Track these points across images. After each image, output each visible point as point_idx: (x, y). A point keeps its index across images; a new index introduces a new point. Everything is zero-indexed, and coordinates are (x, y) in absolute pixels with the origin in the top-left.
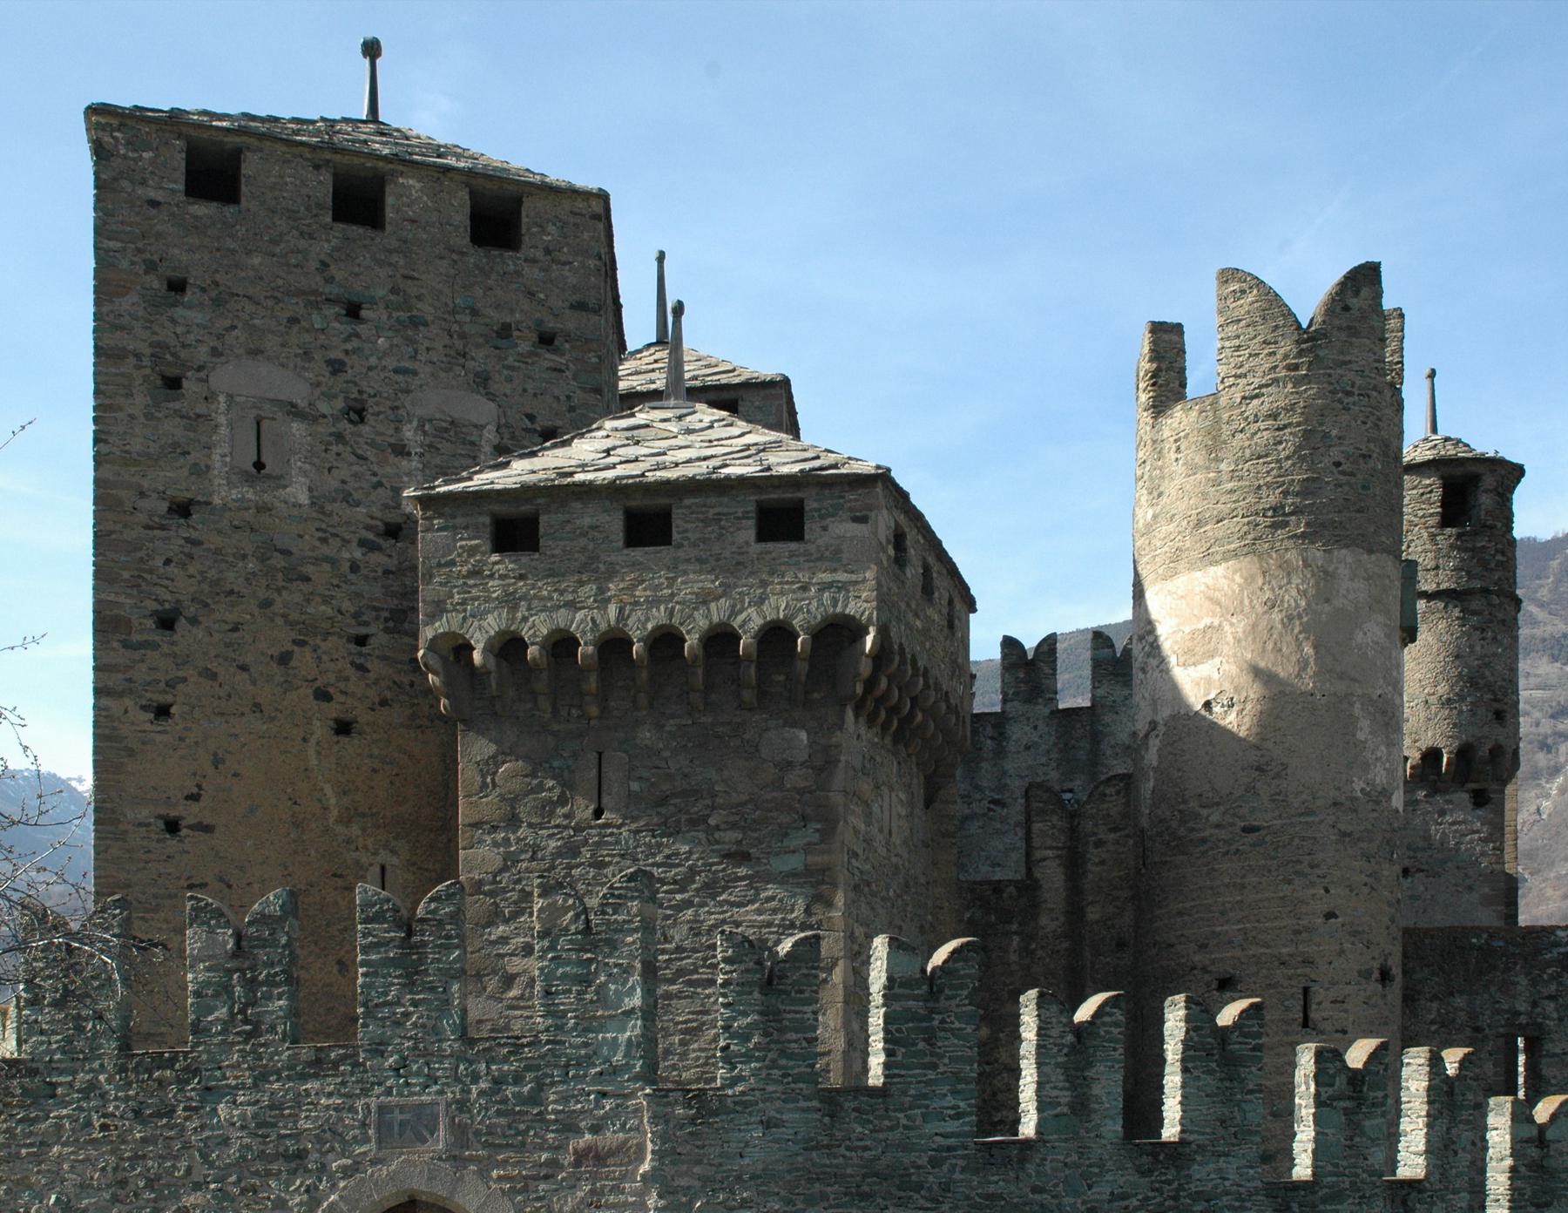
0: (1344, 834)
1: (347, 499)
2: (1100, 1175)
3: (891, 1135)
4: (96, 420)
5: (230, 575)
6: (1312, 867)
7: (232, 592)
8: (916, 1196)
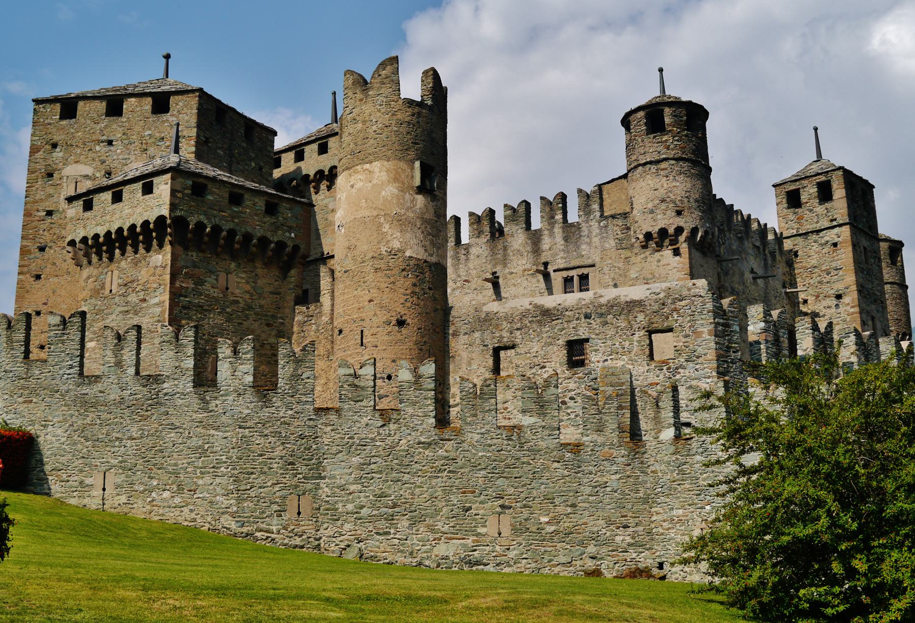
3: (48, 374)
4: (26, 191)
6: (364, 283)
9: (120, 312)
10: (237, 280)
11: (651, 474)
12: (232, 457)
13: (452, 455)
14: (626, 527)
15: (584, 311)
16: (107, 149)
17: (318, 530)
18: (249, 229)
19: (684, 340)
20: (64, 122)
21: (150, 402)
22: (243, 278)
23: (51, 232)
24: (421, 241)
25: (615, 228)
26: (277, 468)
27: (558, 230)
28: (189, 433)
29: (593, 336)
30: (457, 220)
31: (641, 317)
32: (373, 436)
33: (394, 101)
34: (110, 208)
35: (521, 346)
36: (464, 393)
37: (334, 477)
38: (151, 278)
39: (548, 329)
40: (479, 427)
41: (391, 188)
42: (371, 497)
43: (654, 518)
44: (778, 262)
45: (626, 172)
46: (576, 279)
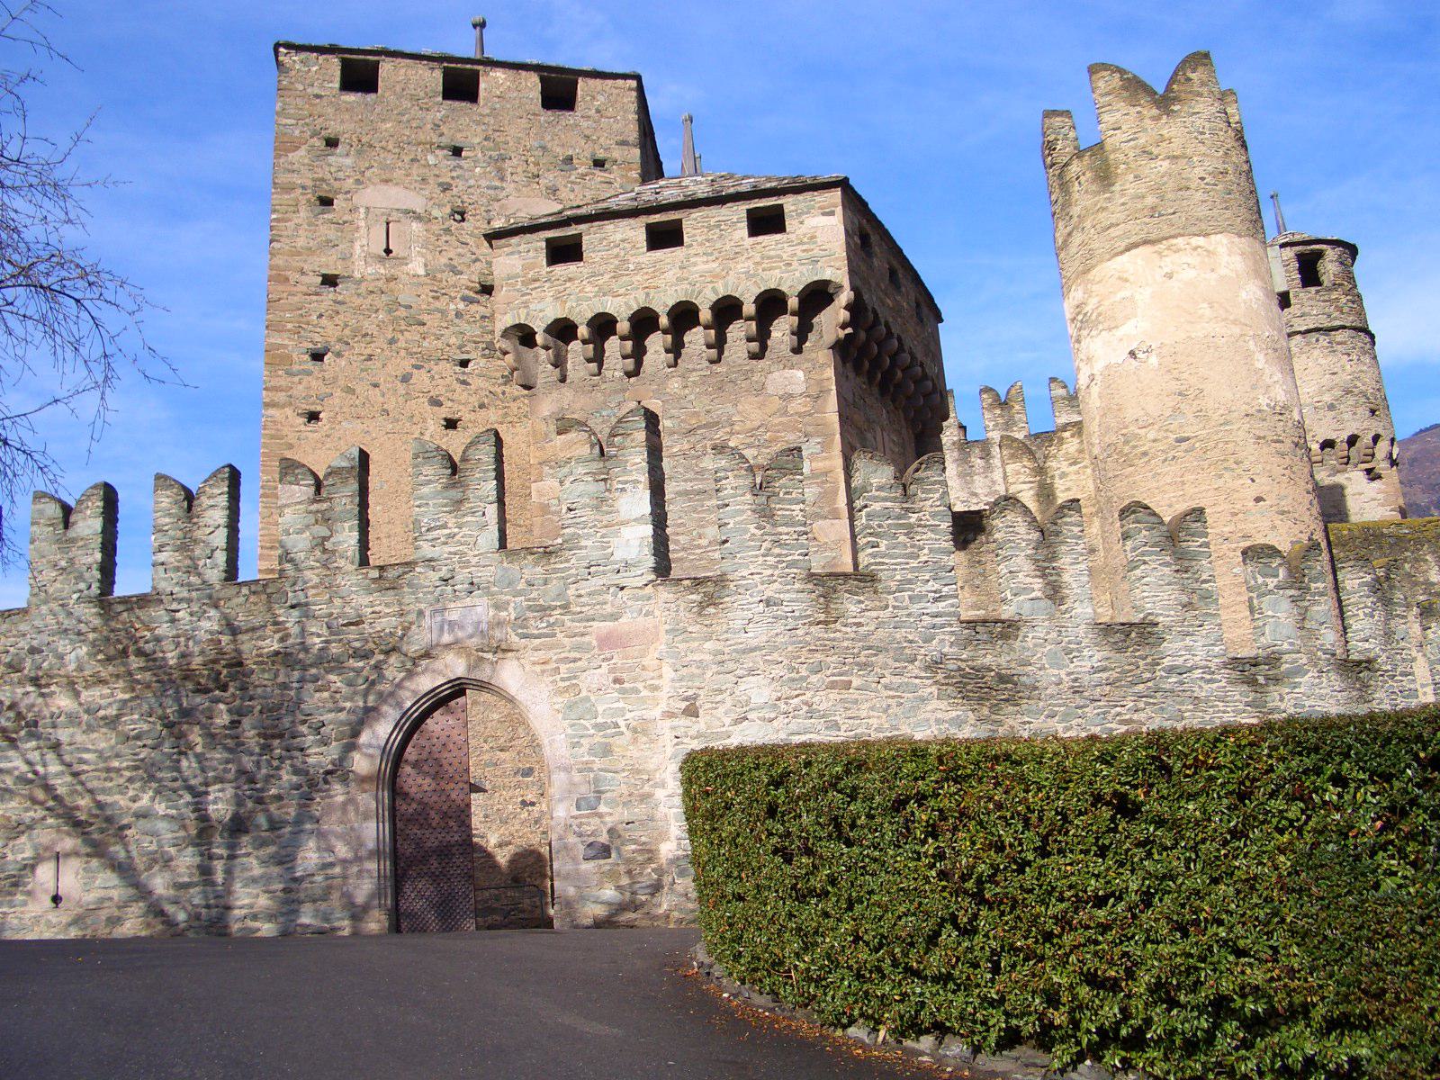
0: (1259, 438)
1: (455, 271)
3: (881, 614)
5: (366, 324)
7: (366, 335)
16: (453, 162)
20: (351, 98)
21: (1141, 687)
23: (339, 319)
34: (640, 259)
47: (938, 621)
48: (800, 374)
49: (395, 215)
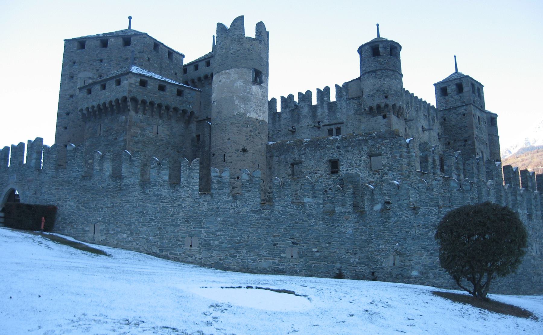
0: (232, 123)
2: (105, 182)
3: (67, 175)
4: (60, 85)
6: (226, 130)
8: (71, 185)
9: (105, 145)
10: (162, 129)
11: (369, 227)
12: (157, 217)
13: (269, 217)
14: (355, 254)
15: (337, 144)
17: (200, 254)
18: (169, 103)
19: (386, 160)
20: (78, 51)
21: (117, 189)
22: (165, 128)
23: (72, 105)
24: (255, 110)
25: (355, 104)
26: (180, 223)
27: (325, 105)
28: (136, 205)
29: (341, 158)
30: (274, 100)
31: (365, 148)
32: (229, 207)
33: (241, 38)
34: (100, 93)
35: (304, 162)
36: (275, 186)
37: (208, 228)
38: (120, 128)
39: (319, 154)
40: (282, 203)
41: (240, 83)
42: (227, 238)
43: (370, 250)
44: (435, 123)
45: (359, 76)
46: (334, 130)
47: (77, 176)
48: (124, 117)
49: (86, 79)
